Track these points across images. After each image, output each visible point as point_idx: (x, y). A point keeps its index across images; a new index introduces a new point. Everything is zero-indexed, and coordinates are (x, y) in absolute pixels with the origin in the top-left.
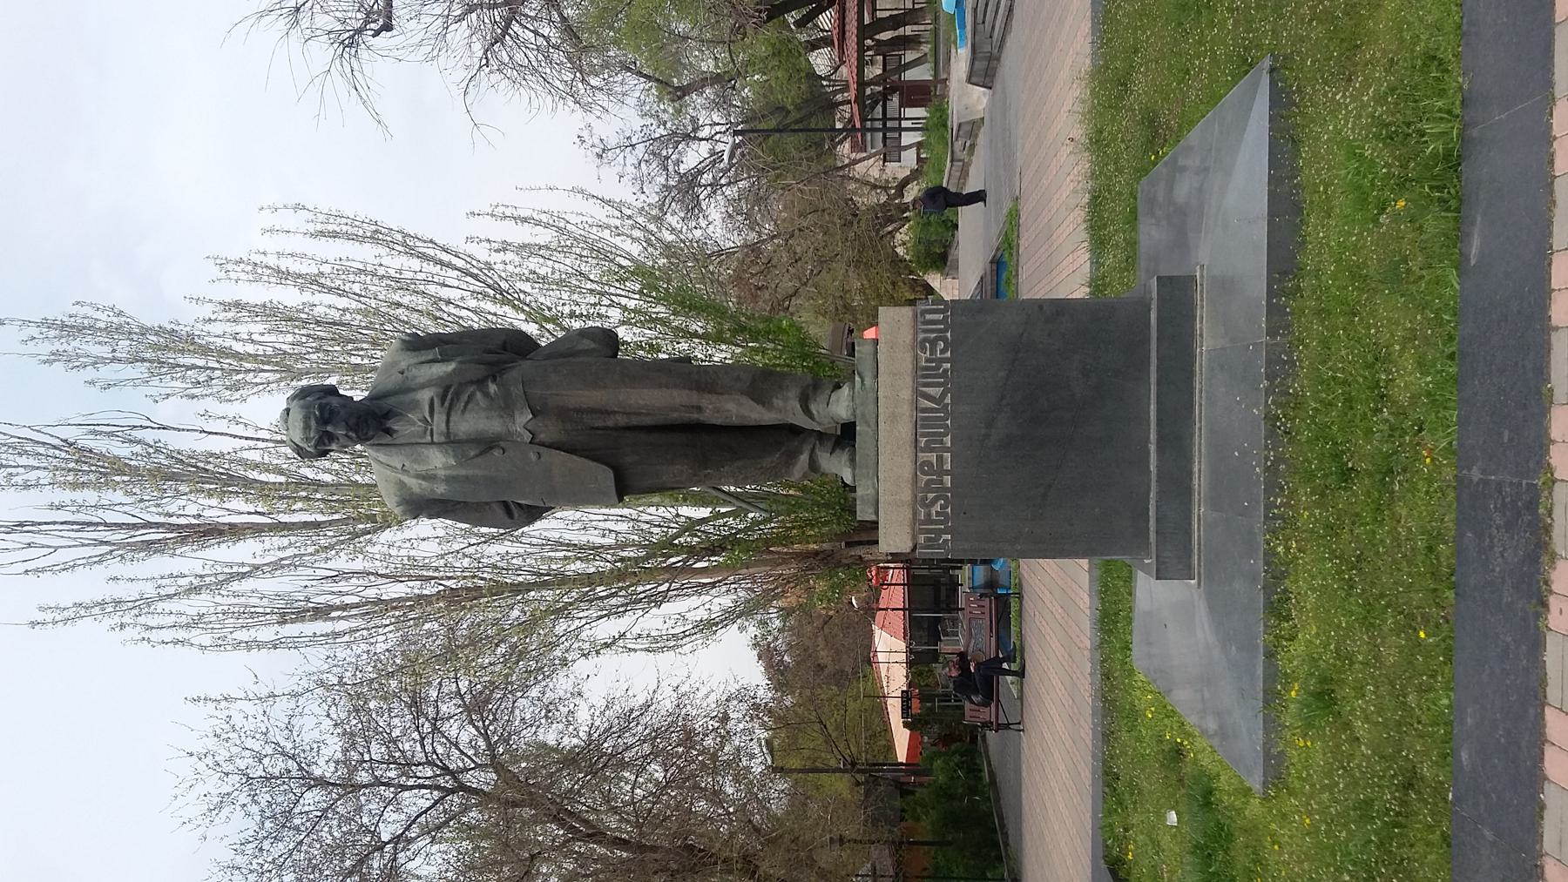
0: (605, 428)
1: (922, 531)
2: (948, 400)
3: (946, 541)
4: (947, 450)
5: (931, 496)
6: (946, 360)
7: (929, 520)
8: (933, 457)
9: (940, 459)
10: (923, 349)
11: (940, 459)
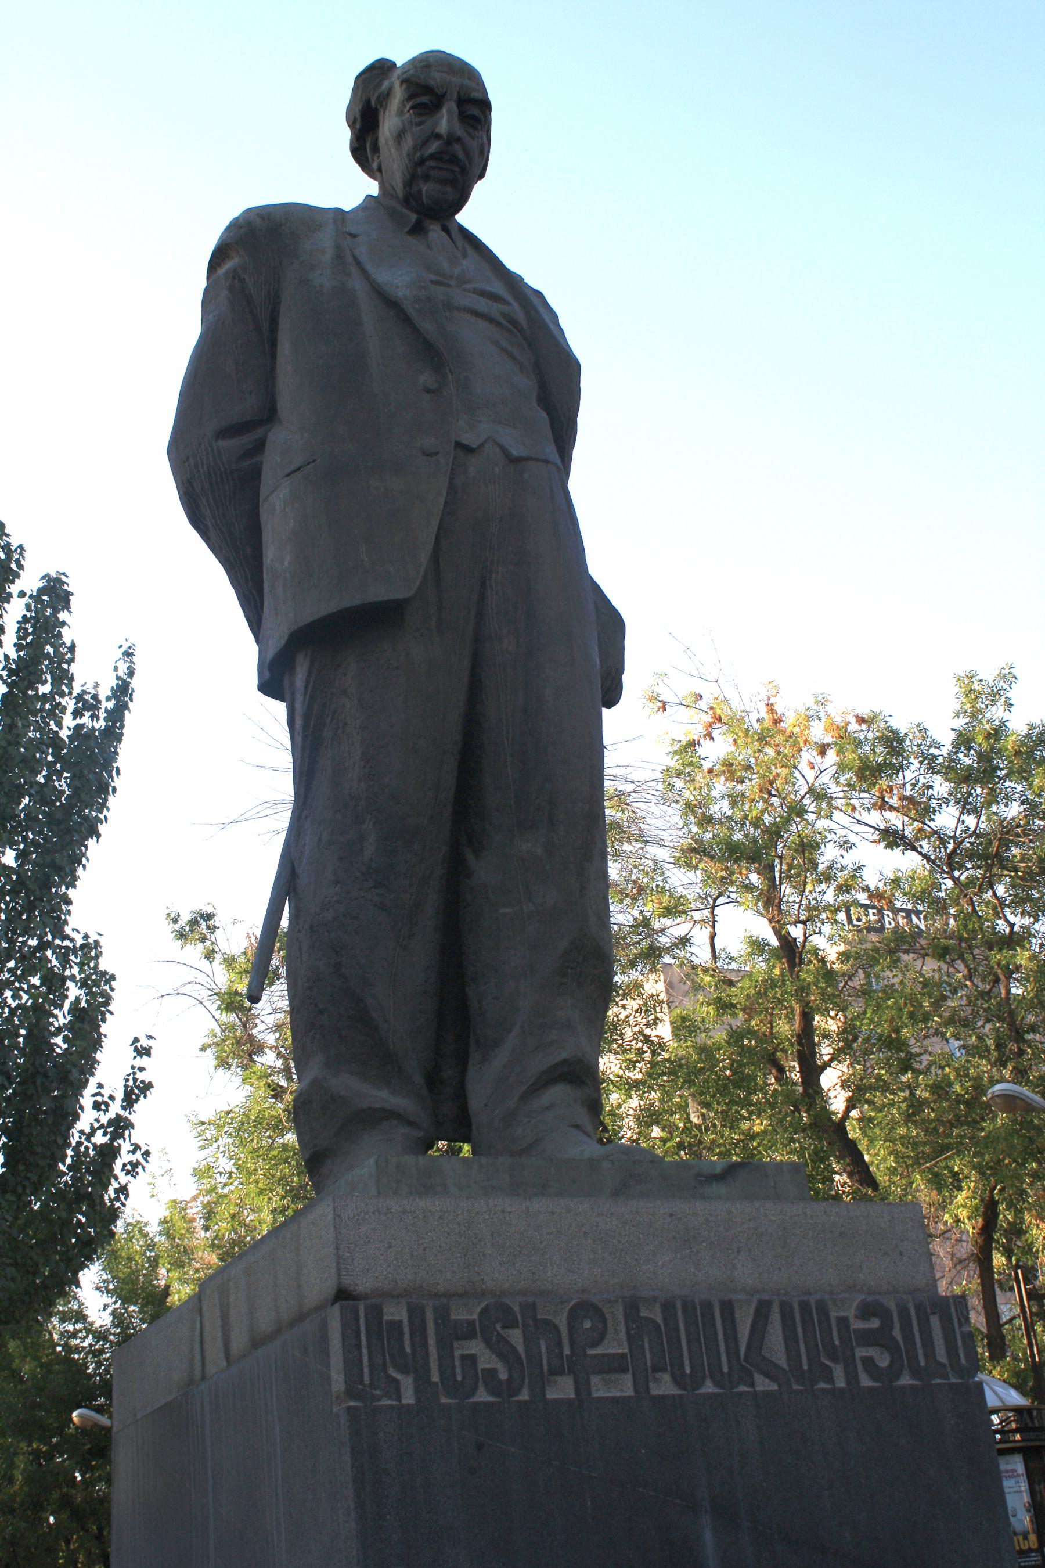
0: (480, 616)
1: (416, 1313)
2: (763, 1384)
3: (395, 1387)
4: (641, 1386)
5: (516, 1337)
6: (852, 1377)
7: (453, 1333)
8: (615, 1345)
9: (615, 1366)
10: (867, 1311)
11: (615, 1366)
